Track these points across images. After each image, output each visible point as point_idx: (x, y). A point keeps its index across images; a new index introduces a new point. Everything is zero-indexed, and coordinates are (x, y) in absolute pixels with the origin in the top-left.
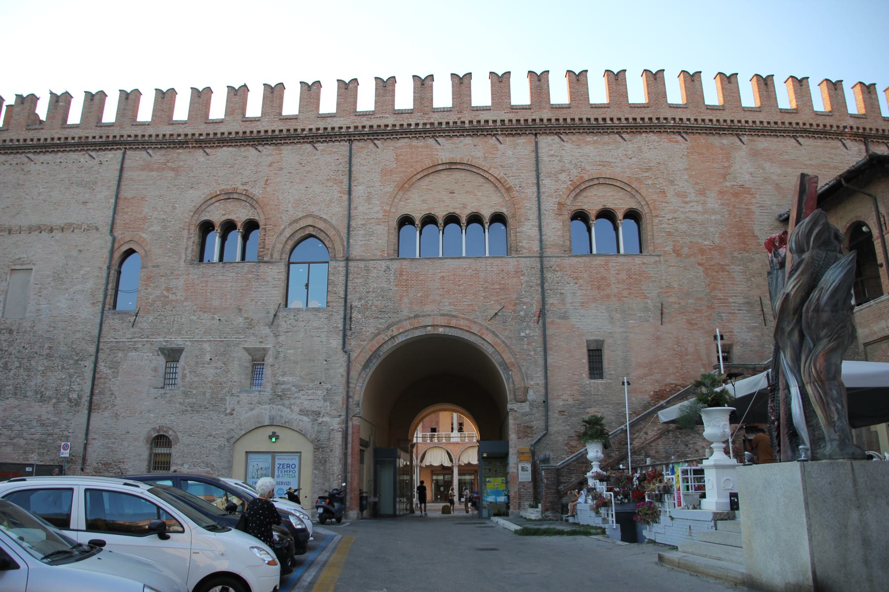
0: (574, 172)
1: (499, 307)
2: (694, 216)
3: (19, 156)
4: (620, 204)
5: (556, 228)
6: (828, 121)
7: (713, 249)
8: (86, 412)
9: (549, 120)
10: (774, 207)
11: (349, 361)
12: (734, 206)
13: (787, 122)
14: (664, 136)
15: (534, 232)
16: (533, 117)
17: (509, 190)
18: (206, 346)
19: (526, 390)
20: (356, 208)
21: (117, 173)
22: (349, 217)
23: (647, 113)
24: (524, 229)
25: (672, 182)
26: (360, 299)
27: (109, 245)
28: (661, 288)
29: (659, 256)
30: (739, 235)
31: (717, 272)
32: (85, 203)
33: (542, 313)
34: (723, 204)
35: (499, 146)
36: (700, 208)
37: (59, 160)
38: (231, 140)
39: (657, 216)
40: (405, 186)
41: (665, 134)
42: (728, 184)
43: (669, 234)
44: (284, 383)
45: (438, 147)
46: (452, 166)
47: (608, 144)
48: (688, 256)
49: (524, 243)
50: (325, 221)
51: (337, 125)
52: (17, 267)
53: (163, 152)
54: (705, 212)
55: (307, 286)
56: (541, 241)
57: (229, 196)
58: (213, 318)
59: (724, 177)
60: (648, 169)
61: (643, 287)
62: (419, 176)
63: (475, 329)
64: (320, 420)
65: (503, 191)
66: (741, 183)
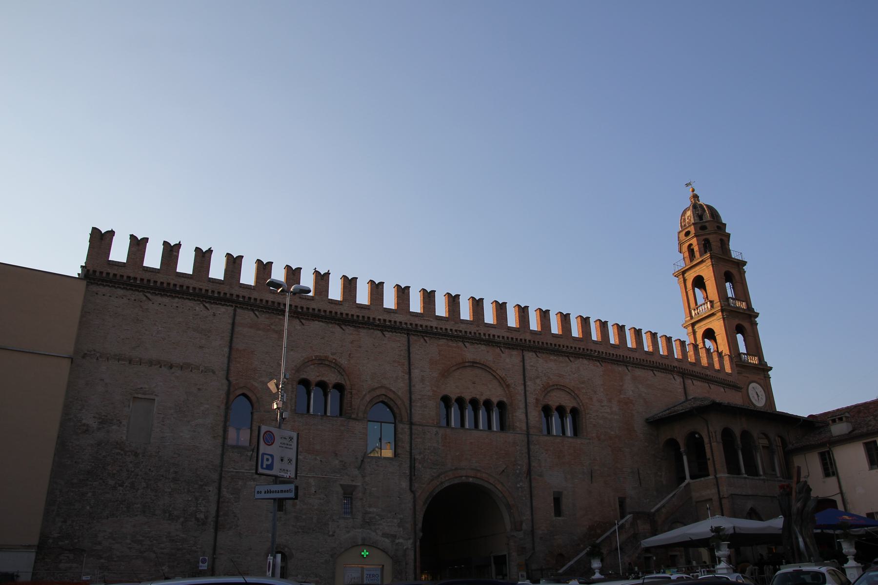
3: (137, 293)
4: (569, 403)
5: (535, 416)
8: (213, 530)
11: (414, 497)
15: (523, 417)
17: (508, 386)
18: (311, 481)
20: (414, 386)
21: (230, 327)
22: (410, 392)
26: (420, 453)
27: (225, 388)
32: (201, 347)
33: (529, 472)
35: (503, 355)
36: (608, 410)
37: (175, 305)
38: (322, 317)
40: (445, 374)
42: (622, 396)
44: (370, 513)
46: (474, 364)
49: (517, 424)
50: (394, 392)
51: (398, 320)
52: (140, 396)
53: (267, 316)
55: (380, 439)
57: (322, 361)
58: (316, 459)
62: (454, 368)
64: (397, 541)
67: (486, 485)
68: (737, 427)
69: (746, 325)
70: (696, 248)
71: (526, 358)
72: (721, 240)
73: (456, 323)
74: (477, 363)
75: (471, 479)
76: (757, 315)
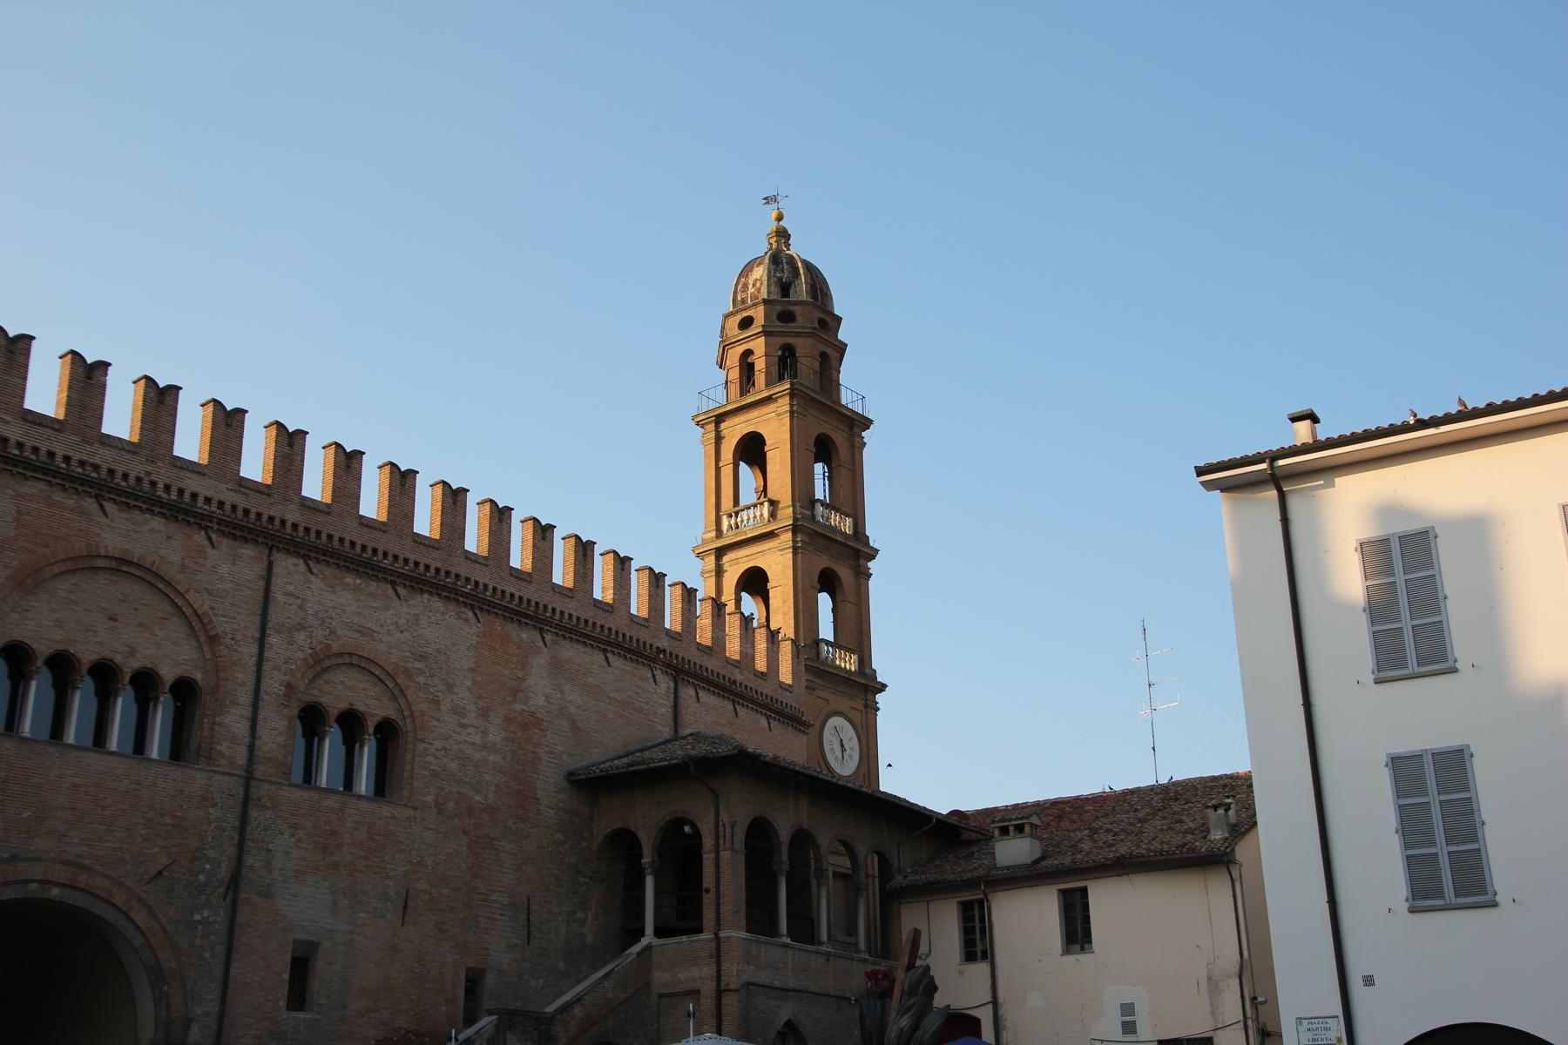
0: (319, 633)
1: (166, 861)
2: (469, 750)
4: (374, 705)
5: (278, 729)
9: (295, 526)
15: (241, 729)
16: (272, 513)
17: (213, 640)
19: (188, 1022)
24: (228, 719)
25: (450, 687)
33: (235, 882)
35: (211, 553)
36: (478, 739)
39: (423, 741)
42: (518, 707)
43: (435, 774)
45: (103, 520)
46: (121, 566)
49: (224, 747)
56: (251, 748)
60: (423, 658)
62: (56, 569)
63: (119, 898)
65: (202, 638)
67: (100, 909)
69: (845, 574)
70: (760, 364)
71: (277, 569)
72: (824, 355)
73: (86, 441)
74: (130, 563)
75: (55, 891)
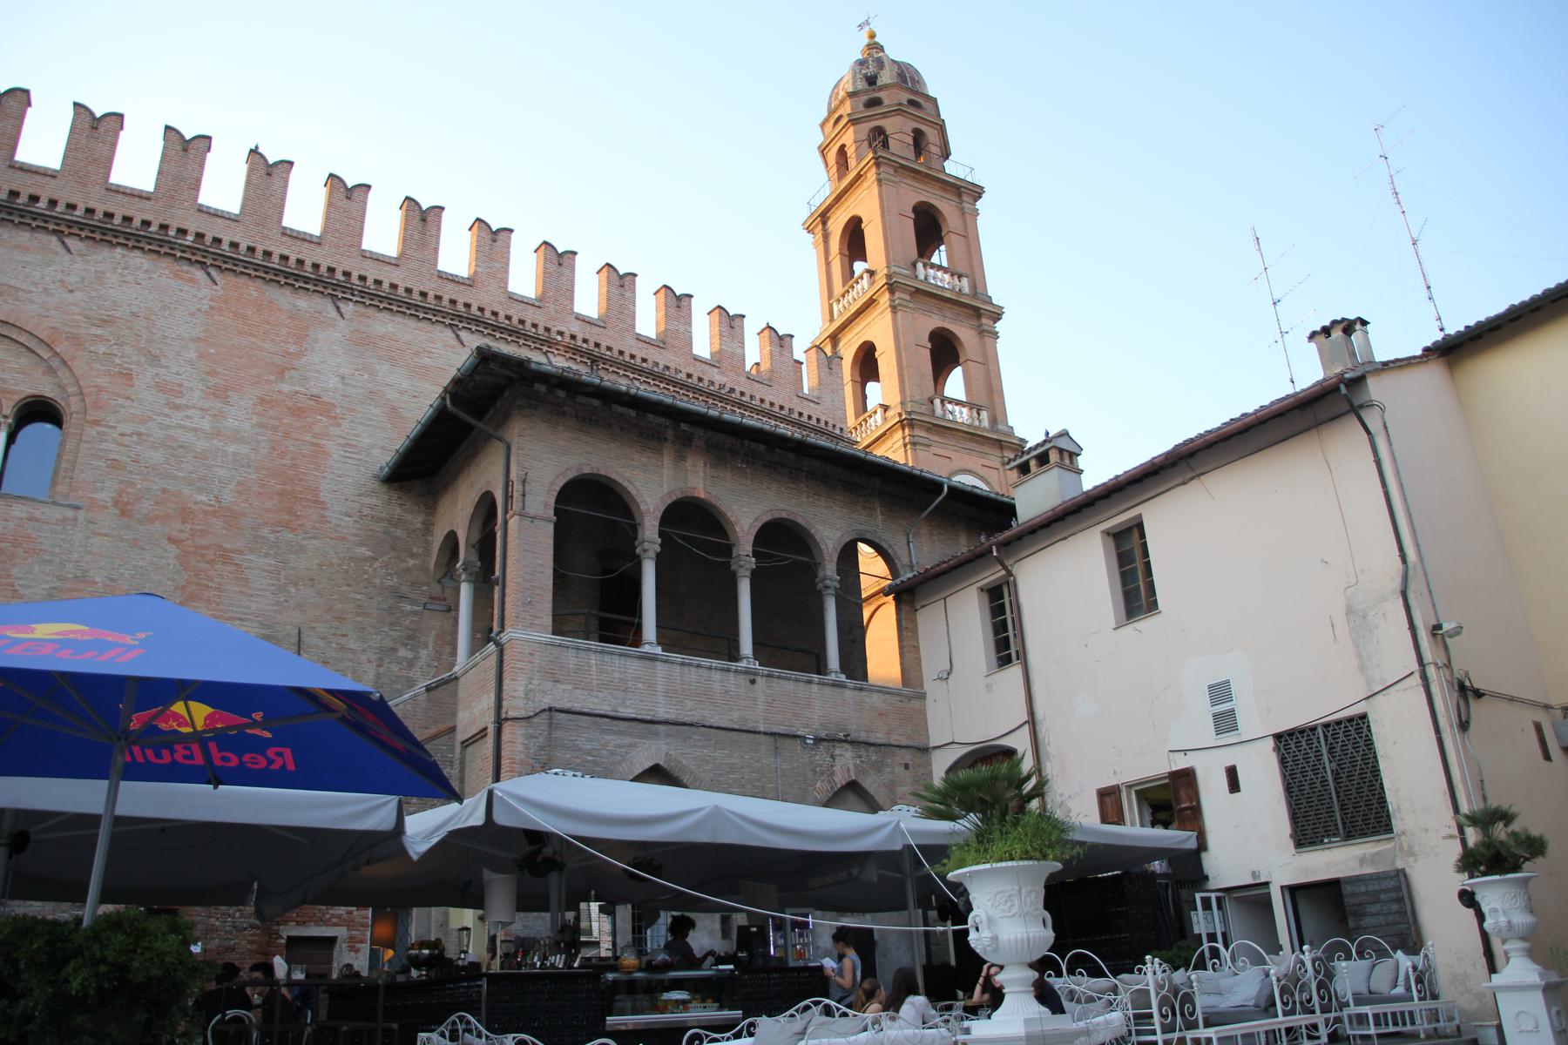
2: (184, 437)
6: (531, 316)
7: (214, 514)
10: (376, 452)
12: (287, 435)
13: (446, 298)
14: (165, 263)
23: (143, 211)
28: (60, 578)
29: (77, 508)
30: (283, 493)
31: (211, 562)
34: (262, 426)
36: (206, 424)
39: (97, 423)
41: (169, 260)
42: (285, 387)
43: (115, 465)
47: (25, 249)
48: (149, 519)
54: (217, 434)
59: (281, 373)
61: (14, 571)
66: (315, 391)
68: (651, 484)
70: (850, 151)
76: (997, 315)
